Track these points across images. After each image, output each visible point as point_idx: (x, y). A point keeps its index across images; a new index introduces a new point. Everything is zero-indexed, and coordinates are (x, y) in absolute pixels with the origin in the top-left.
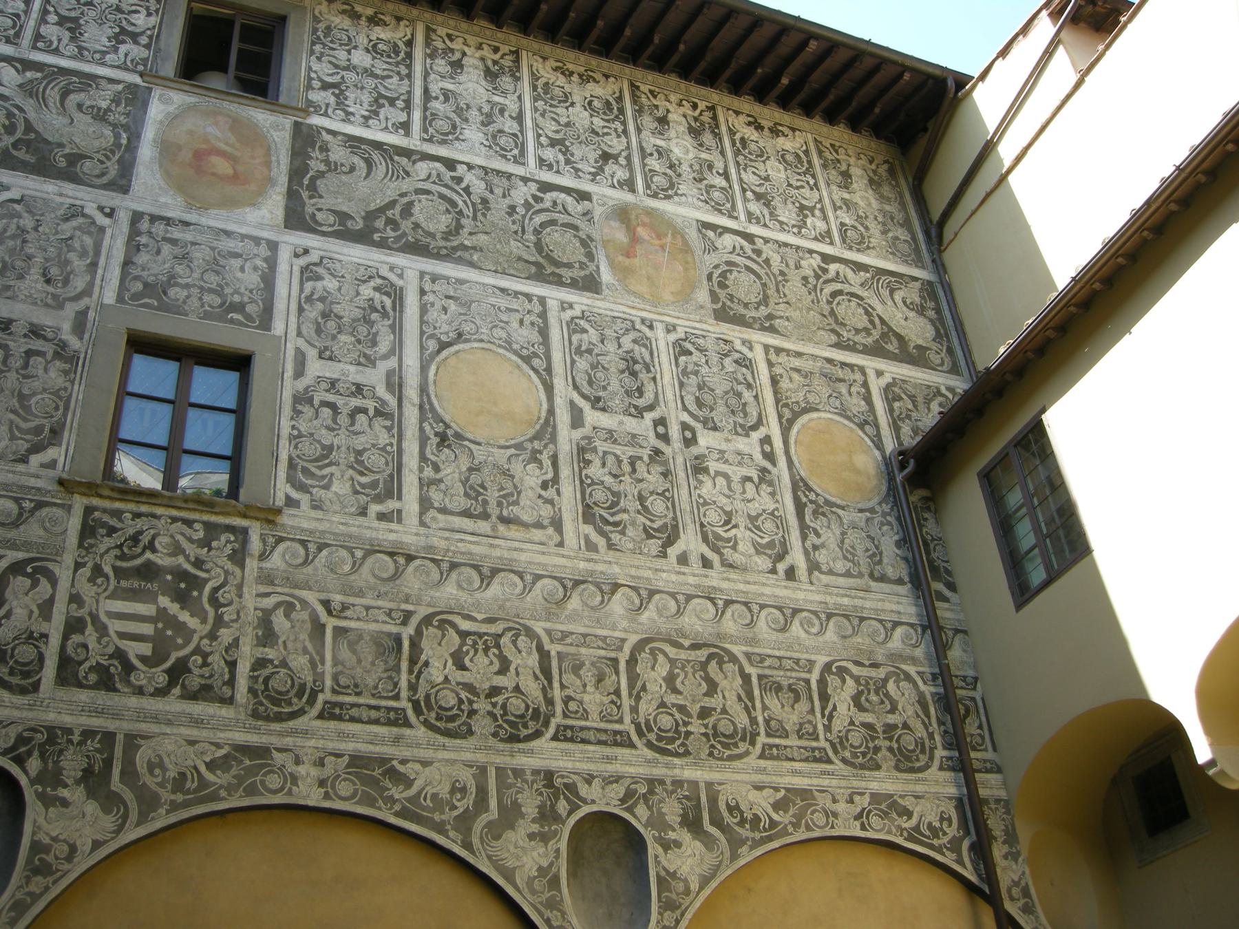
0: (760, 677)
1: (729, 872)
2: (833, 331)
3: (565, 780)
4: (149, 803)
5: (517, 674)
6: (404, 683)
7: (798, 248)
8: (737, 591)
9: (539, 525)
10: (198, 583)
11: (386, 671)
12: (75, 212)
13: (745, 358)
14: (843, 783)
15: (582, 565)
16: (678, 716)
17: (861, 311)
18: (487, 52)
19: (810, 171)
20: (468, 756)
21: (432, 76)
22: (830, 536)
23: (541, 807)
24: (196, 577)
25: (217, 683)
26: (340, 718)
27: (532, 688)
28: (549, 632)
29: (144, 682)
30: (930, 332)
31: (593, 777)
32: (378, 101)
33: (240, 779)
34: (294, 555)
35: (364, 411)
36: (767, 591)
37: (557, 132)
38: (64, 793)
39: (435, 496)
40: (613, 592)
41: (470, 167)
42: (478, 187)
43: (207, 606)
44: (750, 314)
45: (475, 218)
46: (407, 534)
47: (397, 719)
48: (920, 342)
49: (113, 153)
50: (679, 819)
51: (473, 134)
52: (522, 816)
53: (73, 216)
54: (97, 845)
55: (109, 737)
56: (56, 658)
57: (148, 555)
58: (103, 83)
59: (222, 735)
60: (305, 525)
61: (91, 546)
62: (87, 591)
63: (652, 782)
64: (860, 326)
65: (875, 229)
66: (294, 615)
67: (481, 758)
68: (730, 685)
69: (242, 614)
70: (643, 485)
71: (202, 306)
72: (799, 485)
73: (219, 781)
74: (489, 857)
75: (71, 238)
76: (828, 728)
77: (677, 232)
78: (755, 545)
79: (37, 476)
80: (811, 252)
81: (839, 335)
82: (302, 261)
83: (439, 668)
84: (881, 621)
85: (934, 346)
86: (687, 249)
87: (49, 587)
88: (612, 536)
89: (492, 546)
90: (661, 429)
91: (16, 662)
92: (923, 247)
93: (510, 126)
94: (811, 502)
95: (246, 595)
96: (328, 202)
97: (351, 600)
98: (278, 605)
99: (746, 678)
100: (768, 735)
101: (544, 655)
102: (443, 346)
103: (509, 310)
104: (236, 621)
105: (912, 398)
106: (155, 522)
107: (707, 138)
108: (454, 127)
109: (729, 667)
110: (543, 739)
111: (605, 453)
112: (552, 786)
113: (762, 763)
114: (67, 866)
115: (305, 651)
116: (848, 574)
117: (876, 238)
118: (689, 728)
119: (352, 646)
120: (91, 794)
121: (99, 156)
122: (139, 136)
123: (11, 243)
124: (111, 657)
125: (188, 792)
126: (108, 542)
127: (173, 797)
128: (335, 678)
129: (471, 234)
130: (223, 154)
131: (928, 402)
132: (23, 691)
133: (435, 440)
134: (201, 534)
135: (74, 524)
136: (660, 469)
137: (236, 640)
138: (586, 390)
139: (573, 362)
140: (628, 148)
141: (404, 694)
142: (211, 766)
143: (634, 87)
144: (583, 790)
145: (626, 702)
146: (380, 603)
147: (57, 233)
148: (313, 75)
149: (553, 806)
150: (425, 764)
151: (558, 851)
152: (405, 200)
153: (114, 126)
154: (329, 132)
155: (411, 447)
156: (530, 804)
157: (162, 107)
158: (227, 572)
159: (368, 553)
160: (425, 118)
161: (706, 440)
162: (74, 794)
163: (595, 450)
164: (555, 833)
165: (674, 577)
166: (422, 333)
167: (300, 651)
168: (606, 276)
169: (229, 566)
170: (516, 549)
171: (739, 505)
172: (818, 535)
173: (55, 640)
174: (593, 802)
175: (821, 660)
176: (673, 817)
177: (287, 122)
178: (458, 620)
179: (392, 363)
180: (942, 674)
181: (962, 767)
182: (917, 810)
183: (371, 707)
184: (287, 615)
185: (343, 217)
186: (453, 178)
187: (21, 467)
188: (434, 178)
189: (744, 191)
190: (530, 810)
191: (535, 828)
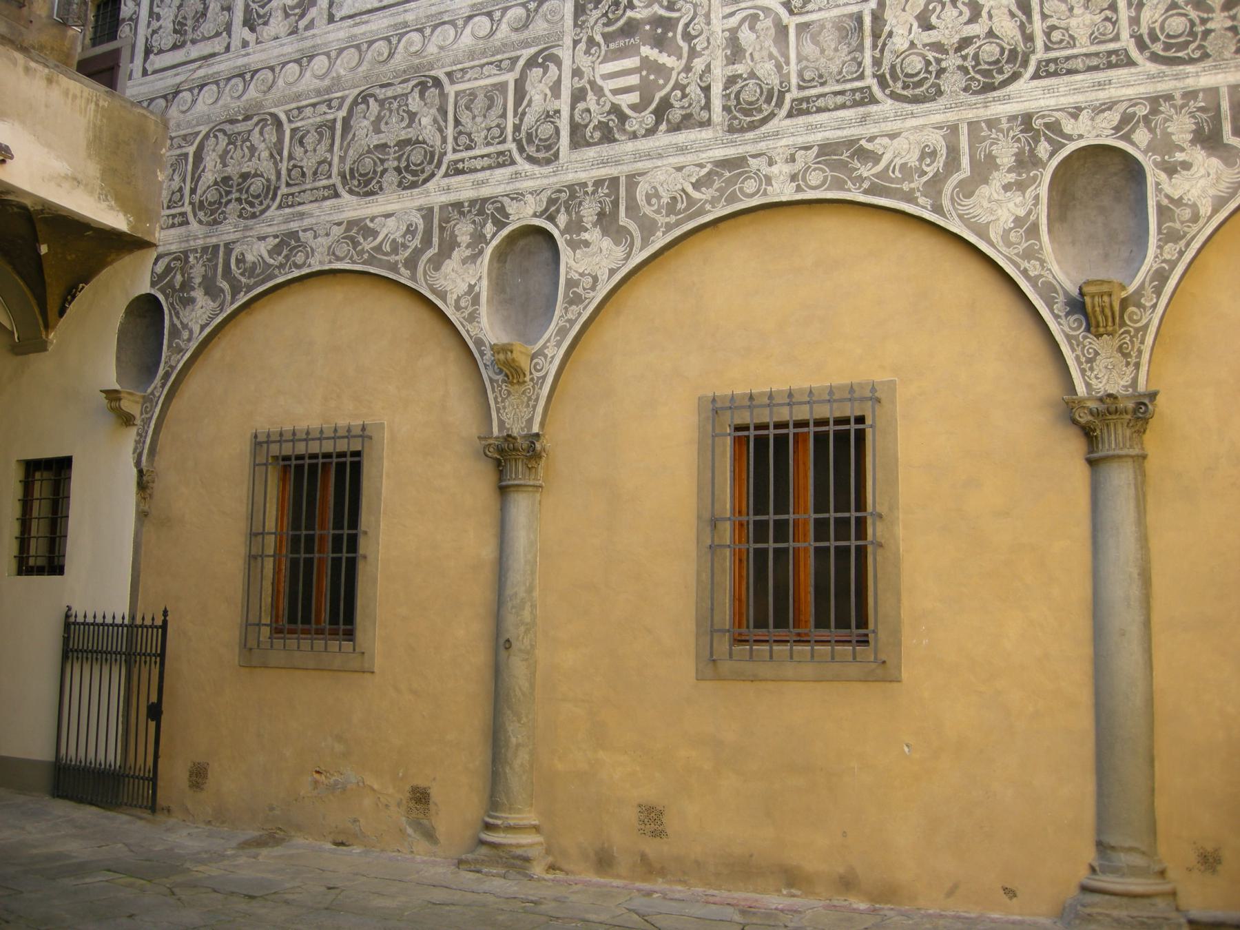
3: (1046, 120)
4: (648, 228)
5: (990, 17)
10: (668, 24)
11: (850, 53)
20: (938, 118)
24: (670, 19)
25: (695, 110)
26: (807, 112)
27: (1008, 29)
31: (1080, 109)
33: (721, 190)
38: (585, 236)
47: (862, 99)
50: (1190, 137)
52: (997, 167)
54: (612, 272)
55: (614, 181)
56: (568, 127)
57: (629, 13)
59: (704, 156)
61: (584, 22)
62: (584, 62)
63: (1155, 101)
66: (759, 26)
67: (951, 117)
69: (712, 40)
73: (704, 197)
74: (960, 217)
87: (556, 69)
91: (540, 140)
95: (714, 21)
110: (1022, 81)
112: (1033, 129)
114: (592, 294)
115: (771, 56)
118: (1210, 25)
120: (605, 232)
124: (609, 113)
125: (680, 213)
126: (596, 14)
127: (667, 220)
128: (800, 75)
132: (548, 162)
137: (708, 66)
141: (869, 72)
142: (696, 186)
144: (1069, 126)
149: (1032, 151)
150: (893, 136)
151: (1037, 197)
156: (1006, 153)
162: (593, 235)
164: (1035, 178)
167: (766, 59)
173: (565, 114)
174: (1081, 136)
183: (836, 93)
184: (752, 28)
190: (1005, 160)
191: (1012, 177)
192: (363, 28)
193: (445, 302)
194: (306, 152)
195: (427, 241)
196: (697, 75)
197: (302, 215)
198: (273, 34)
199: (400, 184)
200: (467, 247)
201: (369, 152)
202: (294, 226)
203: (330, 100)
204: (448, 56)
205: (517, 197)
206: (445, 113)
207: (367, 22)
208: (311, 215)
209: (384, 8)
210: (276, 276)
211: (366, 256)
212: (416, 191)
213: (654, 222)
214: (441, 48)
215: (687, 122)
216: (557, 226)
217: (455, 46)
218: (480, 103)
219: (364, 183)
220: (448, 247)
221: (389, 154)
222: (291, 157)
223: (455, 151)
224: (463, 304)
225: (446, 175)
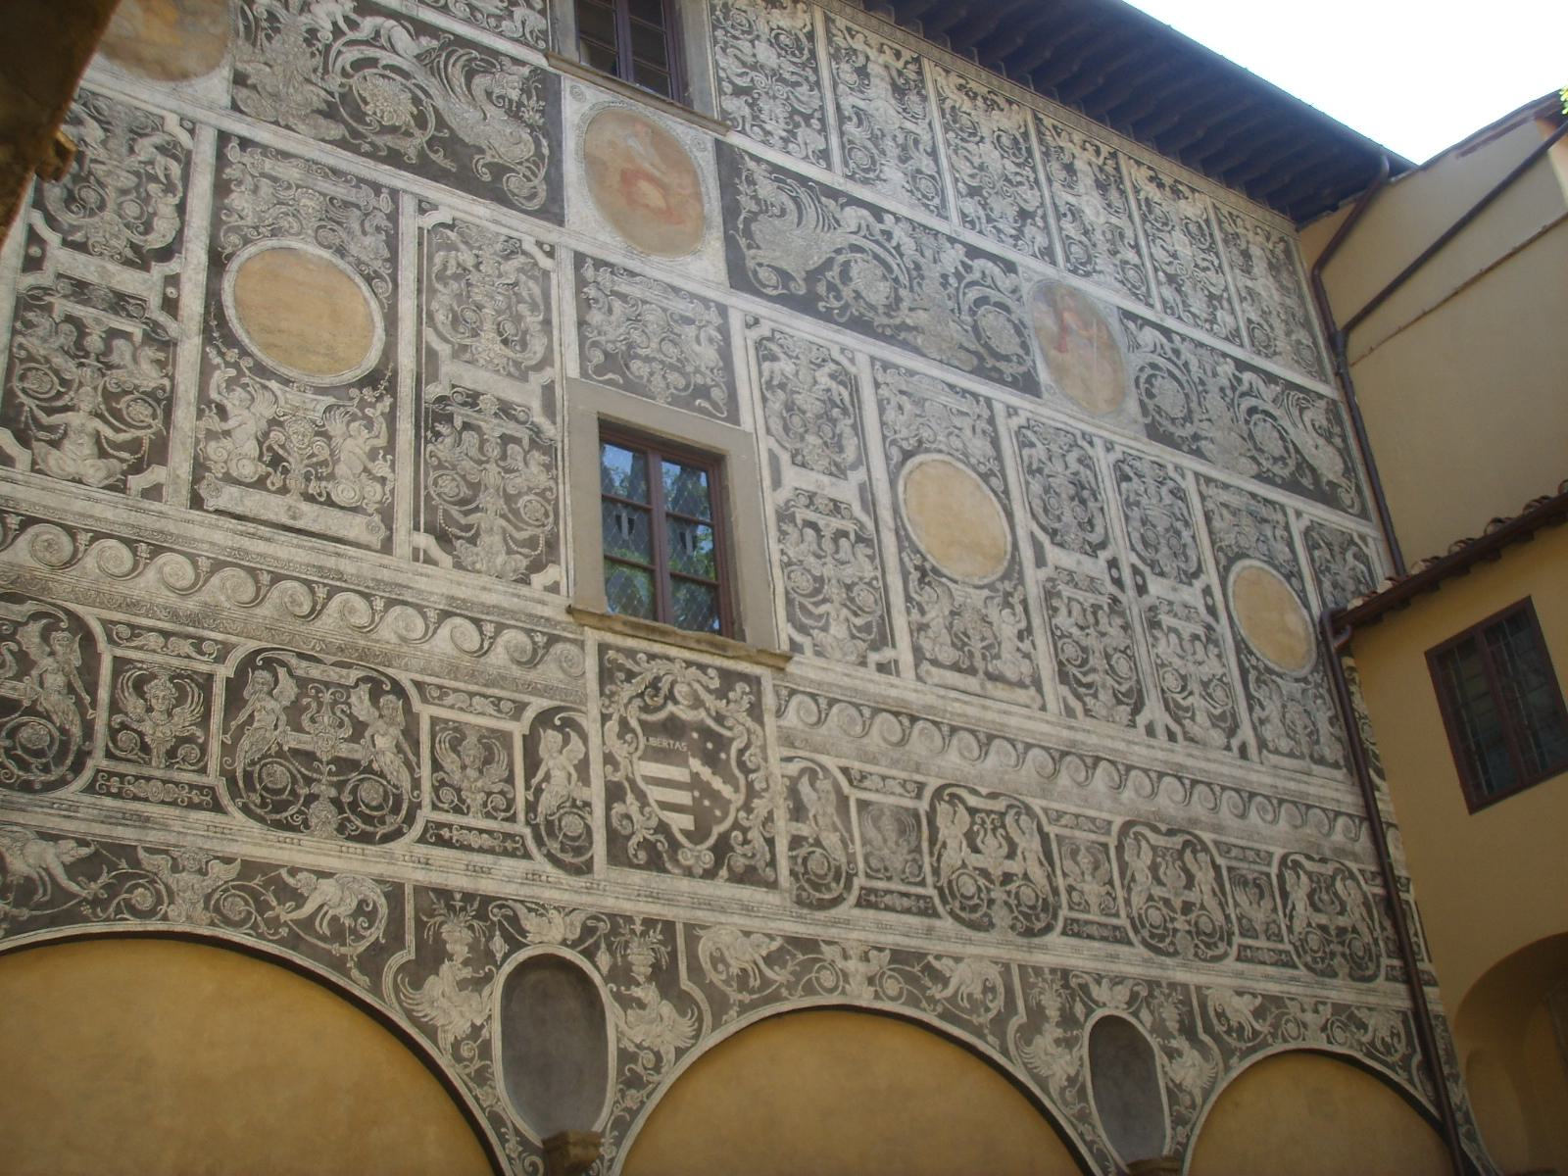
0: (1230, 869)
1: (1224, 1085)
2: (1253, 458)
4: (720, 1005)
6: (927, 869)
7: (1213, 349)
8: (1201, 770)
9: (1021, 684)
10: (722, 743)
11: (910, 852)
12: (512, 249)
13: (1179, 489)
14: (1309, 991)
15: (1065, 733)
16: (1165, 911)
17: (1276, 434)
18: (888, 57)
19: (1211, 248)
20: (992, 951)
21: (841, 87)
22: (1272, 709)
23: (1062, 1010)
25: (760, 864)
26: (875, 906)
27: (1038, 874)
28: (1045, 810)
29: (691, 862)
30: (1340, 467)
32: (797, 118)
34: (808, 712)
35: (846, 534)
36: (1225, 770)
37: (972, 176)
38: (637, 992)
39: (926, 644)
40: (1095, 766)
41: (898, 219)
42: (909, 247)
43: (737, 772)
44: (1179, 432)
45: (911, 289)
46: (903, 688)
48: (1331, 477)
51: (893, 173)
52: (1046, 1019)
54: (680, 1052)
55: (669, 927)
57: (670, 707)
59: (772, 925)
60: (812, 674)
61: (613, 694)
63: (1152, 984)
64: (1277, 454)
65: (1280, 329)
66: (818, 784)
67: (1004, 953)
68: (1205, 878)
70: (1106, 640)
72: (1242, 647)
75: (516, 284)
76: (1290, 929)
77: (1102, 324)
78: (1210, 716)
80: (1225, 355)
81: (1259, 464)
82: (754, 334)
83: (955, 853)
84: (1324, 810)
85: (1344, 482)
86: (1112, 345)
88: (1087, 699)
89: (984, 707)
90: (1114, 572)
92: (1324, 354)
93: (927, 165)
94: (1255, 668)
95: (771, 760)
96: (765, 255)
97: (868, 768)
98: (803, 771)
99: (1217, 868)
100: (1242, 935)
101: (1045, 838)
102: (907, 455)
103: (961, 413)
104: (766, 790)
105: (1329, 545)
106: (669, 665)
107: (1114, 195)
108: (874, 162)
109: (1202, 856)
111: (1070, 599)
113: (1240, 966)
114: (656, 1078)
116: (1291, 755)
117: (1282, 344)
119: (876, 821)
121: (522, 169)
122: (560, 145)
124: (656, 831)
125: (752, 991)
126: (627, 691)
127: (740, 997)
129: (911, 309)
130: (650, 179)
131: (1343, 552)
133: (915, 575)
134: (716, 684)
135: (591, 665)
136: (1119, 621)
137: (771, 813)
138: (1043, 520)
139: (1027, 483)
140: (1042, 204)
141: (930, 880)
142: (769, 960)
143: (1038, 121)
145: (1120, 893)
146: (893, 772)
147: (500, 276)
148: (722, 74)
150: (958, 960)
152: (841, 258)
153: (532, 127)
154: (754, 158)
155: (895, 581)
157: (576, 105)
158: (748, 730)
159: (876, 711)
160: (843, 146)
161: (1157, 587)
162: (647, 993)
163: (1059, 595)
165: (1144, 751)
166: (884, 438)
168: (1044, 376)
169: (749, 723)
171: (1192, 668)
172: (1263, 708)
175: (1278, 852)
176: (1172, 1025)
177: (708, 137)
178: (964, 794)
179: (860, 475)
180: (1385, 871)
181: (1413, 980)
182: (1371, 1023)
184: (812, 785)
185: (785, 276)
186: (883, 232)
187: (524, 590)
188: (864, 232)
189: (1156, 270)
191: (1059, 1033)
192: (260, 547)
193: (435, 1041)
194: (150, 709)
195: (395, 939)
196: (759, 821)
197: (144, 821)
198: (71, 468)
199: (341, 829)
200: (466, 963)
201: (280, 754)
202: (127, 834)
203: (202, 640)
204: (415, 657)
205: (539, 909)
206: (416, 744)
207: (268, 540)
208: (165, 828)
209: (299, 531)
210: (86, 920)
211: (284, 932)
212: (371, 849)
213: (725, 996)
214: (404, 639)
215: (747, 876)
216: (597, 968)
217: (426, 647)
218: (471, 747)
219: (279, 810)
220: (431, 956)
221: (318, 771)
222: (115, 707)
223: (435, 807)
224: (465, 1052)
225: (422, 840)
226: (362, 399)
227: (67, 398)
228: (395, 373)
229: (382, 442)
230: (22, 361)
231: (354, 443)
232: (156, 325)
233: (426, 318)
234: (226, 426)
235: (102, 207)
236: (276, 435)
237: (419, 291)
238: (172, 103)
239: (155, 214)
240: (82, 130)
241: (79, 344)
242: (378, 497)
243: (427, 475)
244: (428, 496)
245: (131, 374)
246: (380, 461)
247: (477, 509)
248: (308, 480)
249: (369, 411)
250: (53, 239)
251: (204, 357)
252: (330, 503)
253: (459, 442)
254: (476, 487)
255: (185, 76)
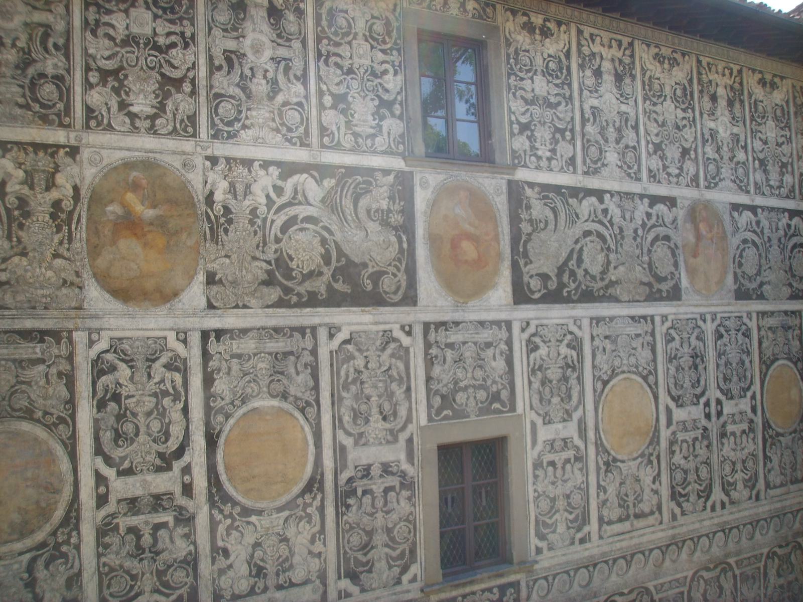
12: (388, 338)
49: (400, 260)
53: (387, 343)
58: (379, 175)
71: (477, 404)
79: (408, 591)
123: (353, 388)
133: (603, 468)
134: (497, 596)
153: (396, 229)
170: (642, 536)
175: (765, 551)
187: (398, 588)
226: (305, 503)
227: (136, 587)
228: (322, 475)
229: (317, 528)
230: (107, 575)
231: (301, 535)
232: (181, 508)
233: (337, 423)
234: (229, 562)
235: (137, 435)
236: (259, 553)
237: (333, 404)
238: (170, 323)
239: (170, 422)
240: (117, 374)
241: (138, 547)
242: (317, 568)
243: (343, 538)
244: (345, 553)
245: (171, 552)
246: (318, 542)
247: (372, 548)
248: (278, 575)
249: (309, 510)
250: (110, 473)
251: (211, 515)
252: (292, 585)
253: (360, 507)
254: (370, 534)
255: (176, 294)
